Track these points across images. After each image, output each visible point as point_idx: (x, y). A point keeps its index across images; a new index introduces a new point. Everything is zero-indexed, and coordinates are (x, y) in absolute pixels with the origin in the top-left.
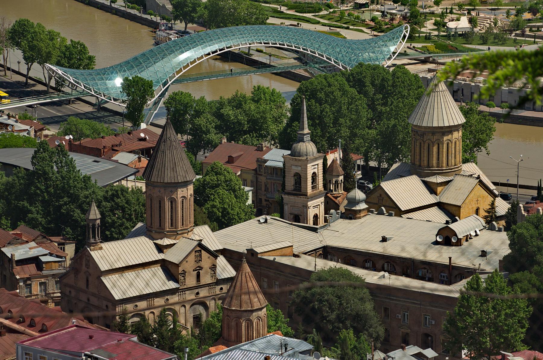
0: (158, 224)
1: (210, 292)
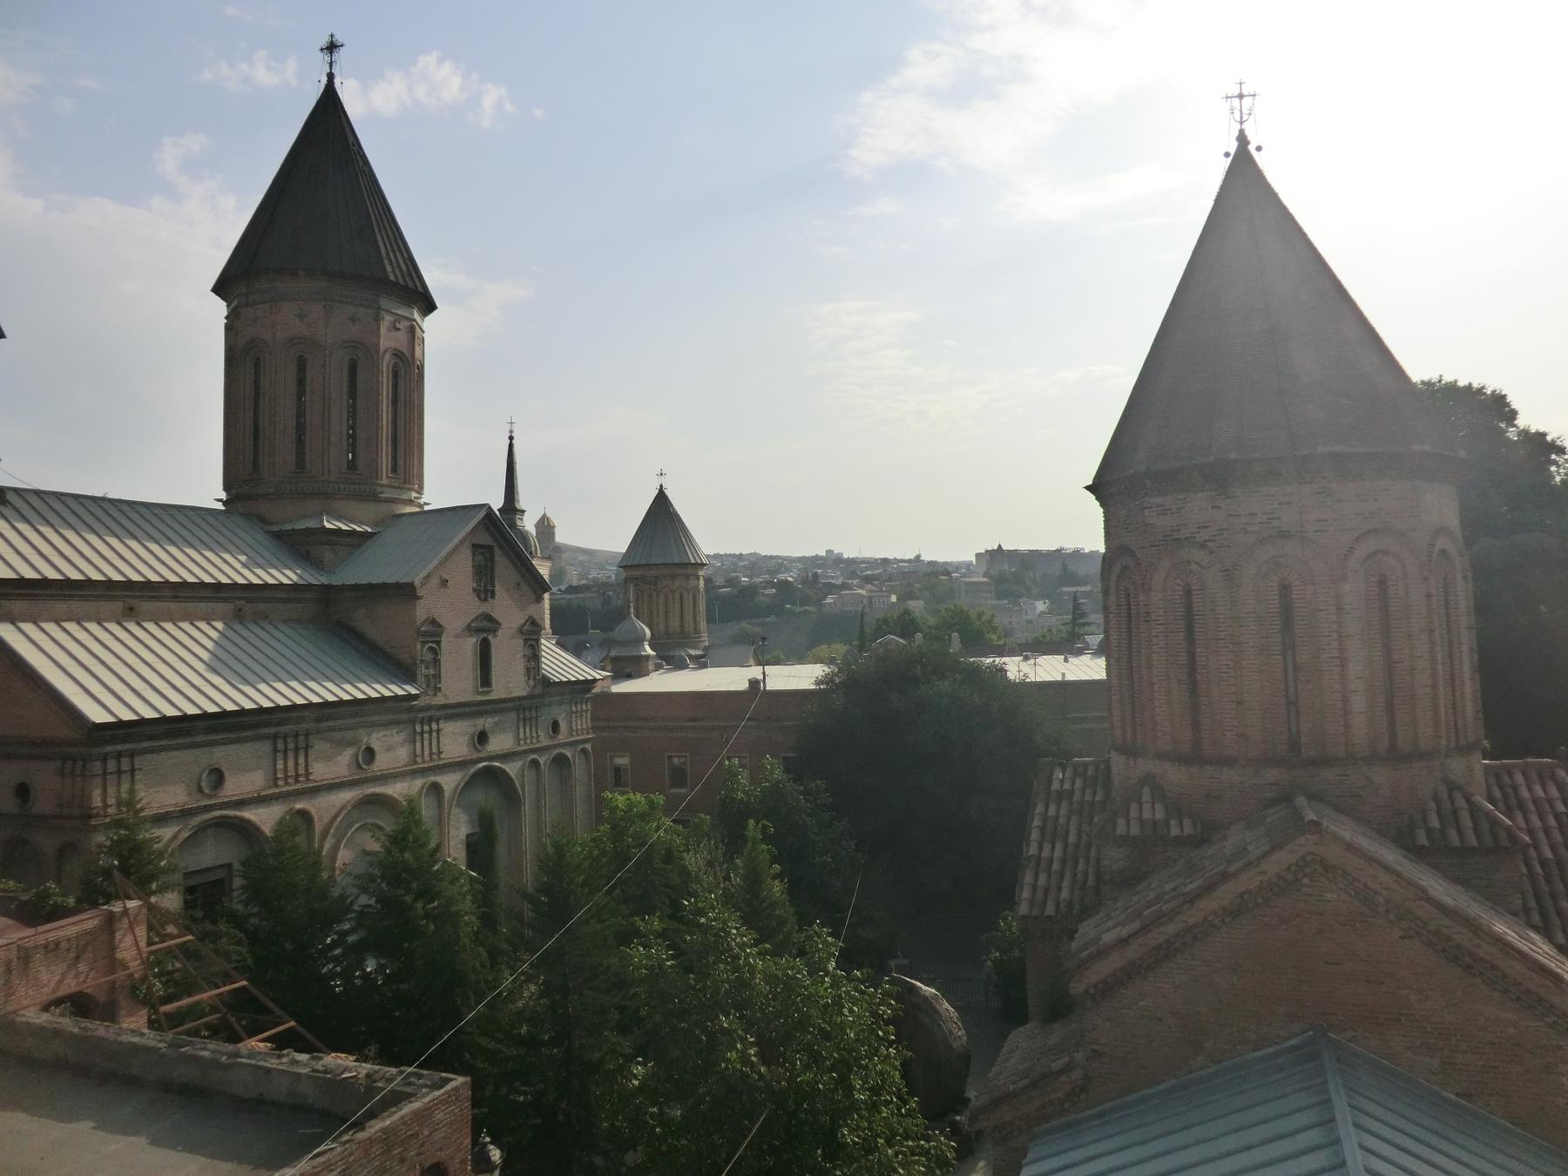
1: (522, 736)
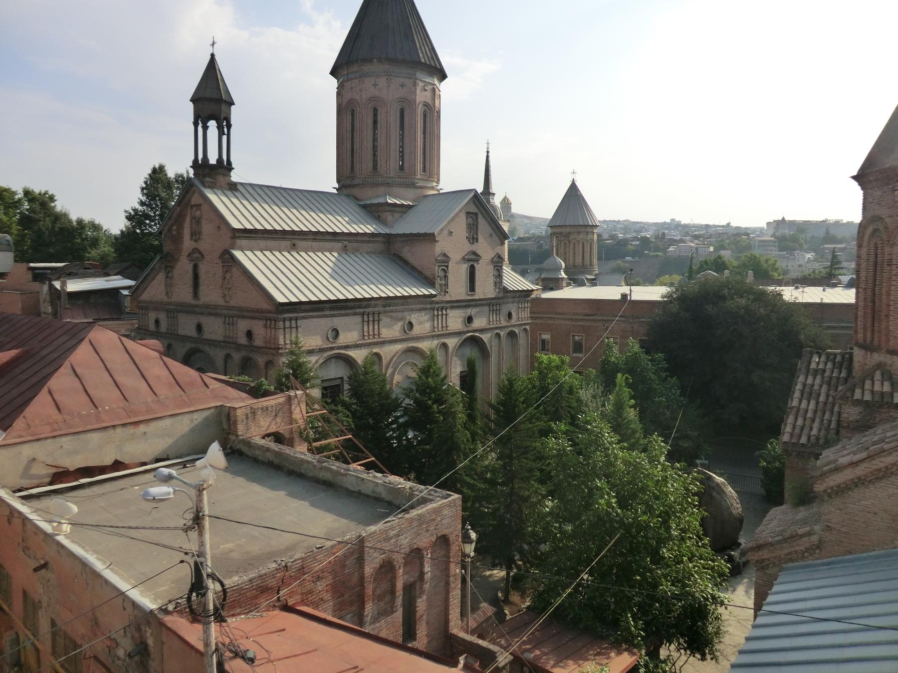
0: (371, 165)
1: (491, 320)
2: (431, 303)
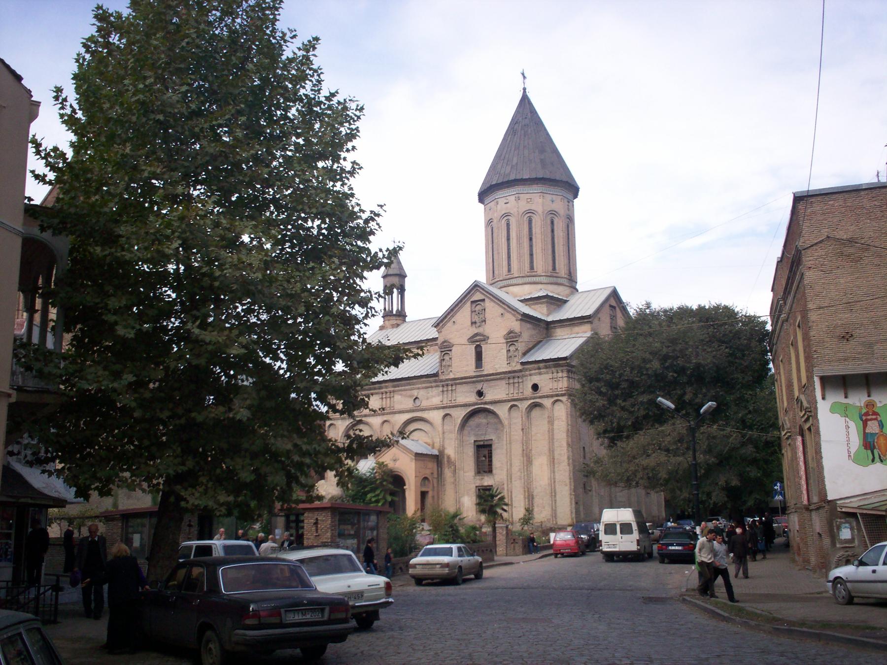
2: (435, 381)
